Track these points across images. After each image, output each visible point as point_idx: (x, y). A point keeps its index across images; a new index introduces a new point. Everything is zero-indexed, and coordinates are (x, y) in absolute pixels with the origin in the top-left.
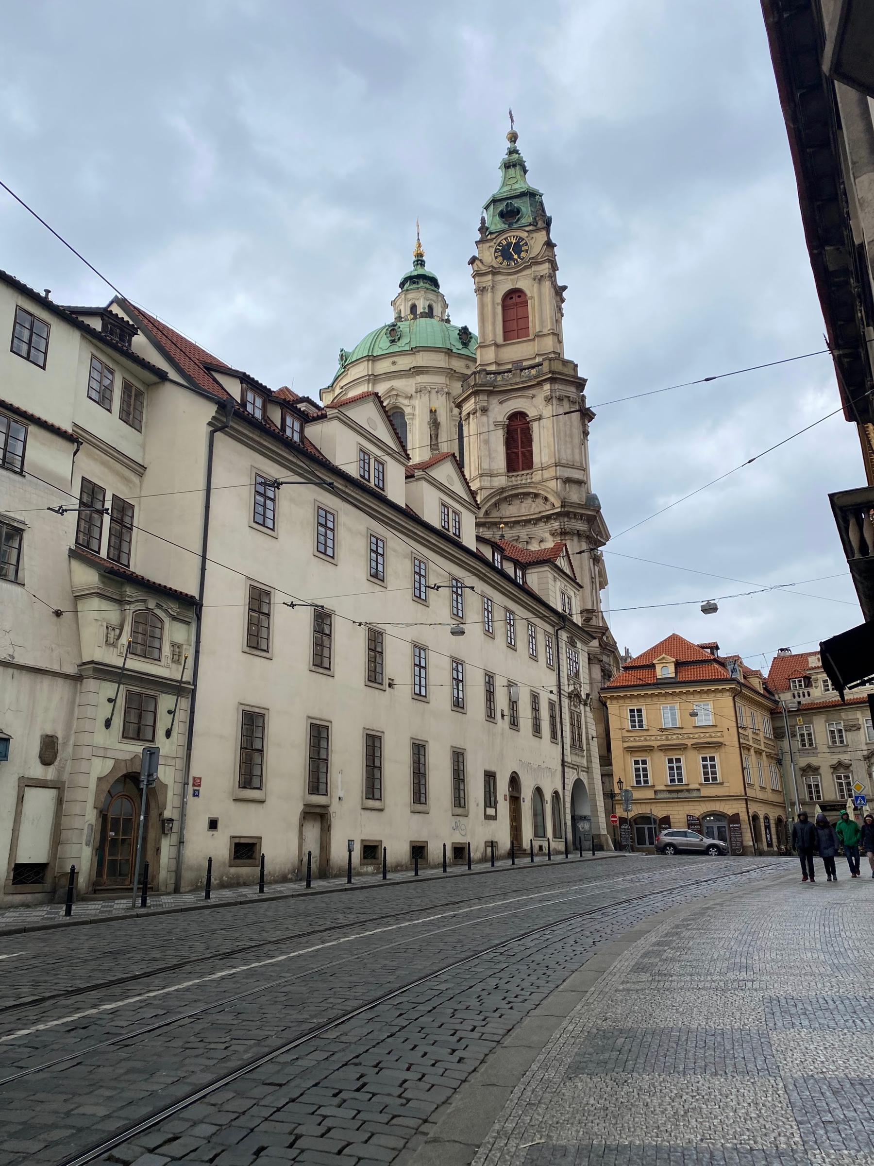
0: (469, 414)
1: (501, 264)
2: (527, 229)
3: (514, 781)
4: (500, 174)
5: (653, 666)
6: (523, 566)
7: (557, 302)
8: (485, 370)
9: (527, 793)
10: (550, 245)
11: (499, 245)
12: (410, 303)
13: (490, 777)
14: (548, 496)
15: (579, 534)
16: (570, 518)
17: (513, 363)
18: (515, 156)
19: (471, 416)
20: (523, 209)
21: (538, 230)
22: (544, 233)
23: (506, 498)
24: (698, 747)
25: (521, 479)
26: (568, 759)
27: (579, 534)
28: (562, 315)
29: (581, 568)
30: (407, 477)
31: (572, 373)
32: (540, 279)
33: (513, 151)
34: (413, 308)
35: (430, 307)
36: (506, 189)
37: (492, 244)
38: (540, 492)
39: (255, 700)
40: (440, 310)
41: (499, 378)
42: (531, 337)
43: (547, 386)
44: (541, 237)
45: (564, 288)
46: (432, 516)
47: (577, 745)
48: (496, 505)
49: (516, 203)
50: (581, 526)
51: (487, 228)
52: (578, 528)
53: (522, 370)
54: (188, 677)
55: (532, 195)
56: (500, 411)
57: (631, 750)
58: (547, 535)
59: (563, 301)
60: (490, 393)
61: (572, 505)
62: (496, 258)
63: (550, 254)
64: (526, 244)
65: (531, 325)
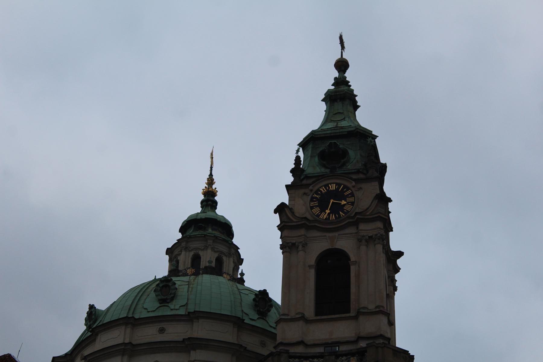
1: (318, 216)
2: (354, 177)
4: (323, 106)
7: (388, 271)
8: (287, 352)
12: (192, 253)
17: (325, 345)
18: (344, 88)
20: (351, 153)
21: (368, 180)
22: (376, 184)
28: (395, 289)
33: (341, 82)
34: (196, 259)
35: (219, 261)
36: (330, 125)
37: (307, 191)
40: (232, 265)
42: (352, 314)
44: (371, 189)
45: (400, 254)
49: (342, 144)
51: (303, 170)
62: (312, 208)
64: (352, 195)
65: (353, 297)
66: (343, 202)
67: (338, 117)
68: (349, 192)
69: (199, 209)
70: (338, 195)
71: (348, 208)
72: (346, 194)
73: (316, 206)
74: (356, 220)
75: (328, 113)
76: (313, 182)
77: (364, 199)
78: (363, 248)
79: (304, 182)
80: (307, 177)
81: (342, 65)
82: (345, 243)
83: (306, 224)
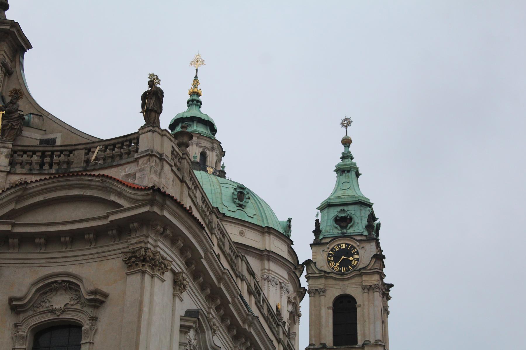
2: (359, 238)
4: (335, 174)
10: (379, 257)
11: (332, 250)
18: (348, 161)
32: (370, 289)
33: (347, 156)
36: (340, 193)
37: (325, 248)
55: (366, 204)
64: (357, 253)
66: (351, 259)
68: (355, 250)
70: (348, 252)
71: (354, 263)
72: (353, 252)
73: (332, 261)
74: (361, 272)
75: (338, 184)
76: (330, 242)
77: (365, 254)
78: (366, 294)
79: (323, 241)
83: (326, 275)
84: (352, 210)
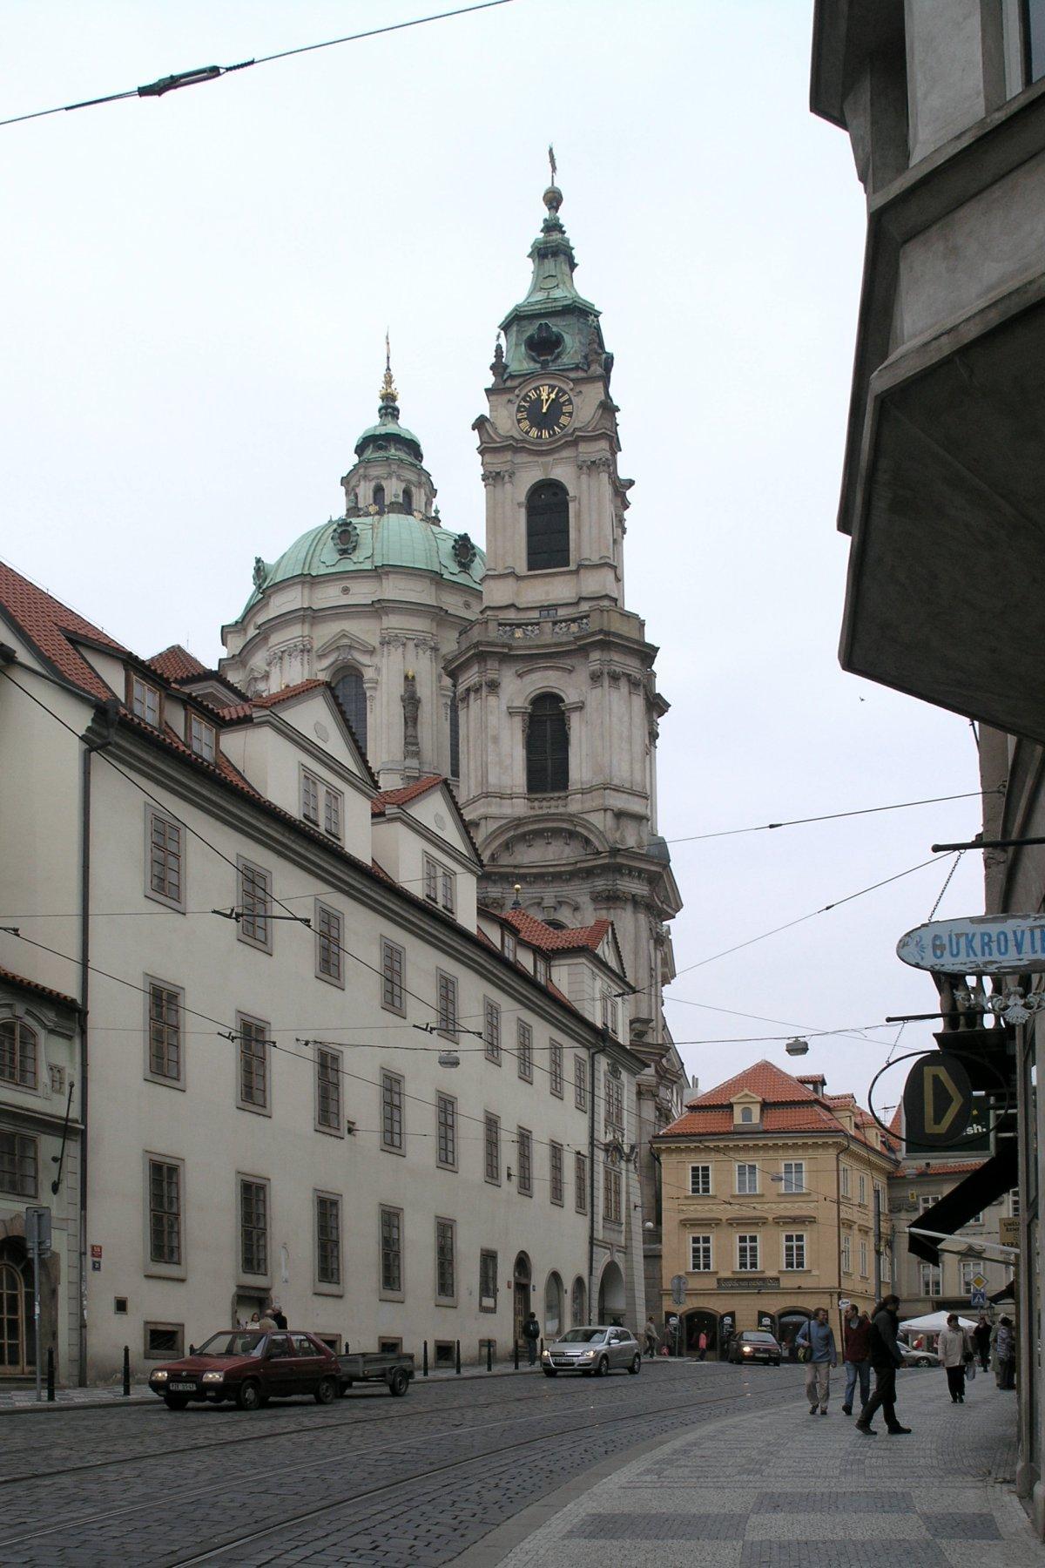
0: (468, 690)
2: (573, 375)
3: (522, 1263)
5: (730, 1106)
6: (547, 956)
9: (539, 1280)
13: (489, 1259)
14: (591, 837)
15: (635, 901)
16: (622, 875)
17: (541, 608)
18: (556, 236)
19: (472, 695)
20: (567, 338)
21: (591, 380)
22: (600, 385)
23: (524, 835)
24: (781, 1221)
25: (550, 806)
26: (600, 1234)
27: (635, 901)
28: (624, 532)
29: (636, 954)
30: (374, 815)
31: (634, 635)
33: (552, 227)
36: (540, 296)
37: (511, 397)
38: (579, 829)
39: (165, 1147)
41: (519, 633)
42: (573, 567)
43: (595, 655)
44: (593, 393)
45: (631, 483)
46: (410, 876)
47: (612, 1218)
48: (507, 846)
50: (638, 888)
51: (506, 367)
52: (634, 891)
53: (555, 623)
54: (75, 1113)
56: (517, 689)
57: (686, 1223)
58: (585, 901)
59: (626, 505)
60: (506, 658)
61: (628, 853)
62: (519, 421)
63: (608, 425)
64: (570, 401)
67: (551, 283)
69: (376, 420)
75: (537, 274)
78: (584, 477)
79: (509, 384)
80: (512, 377)
81: (553, 199)
82: (562, 472)
83: (514, 447)
84: (556, 325)
